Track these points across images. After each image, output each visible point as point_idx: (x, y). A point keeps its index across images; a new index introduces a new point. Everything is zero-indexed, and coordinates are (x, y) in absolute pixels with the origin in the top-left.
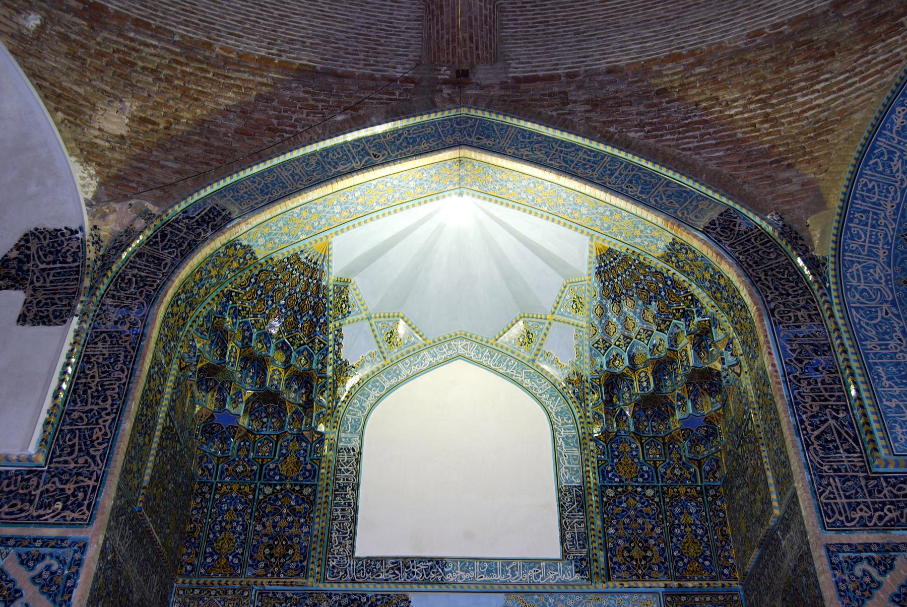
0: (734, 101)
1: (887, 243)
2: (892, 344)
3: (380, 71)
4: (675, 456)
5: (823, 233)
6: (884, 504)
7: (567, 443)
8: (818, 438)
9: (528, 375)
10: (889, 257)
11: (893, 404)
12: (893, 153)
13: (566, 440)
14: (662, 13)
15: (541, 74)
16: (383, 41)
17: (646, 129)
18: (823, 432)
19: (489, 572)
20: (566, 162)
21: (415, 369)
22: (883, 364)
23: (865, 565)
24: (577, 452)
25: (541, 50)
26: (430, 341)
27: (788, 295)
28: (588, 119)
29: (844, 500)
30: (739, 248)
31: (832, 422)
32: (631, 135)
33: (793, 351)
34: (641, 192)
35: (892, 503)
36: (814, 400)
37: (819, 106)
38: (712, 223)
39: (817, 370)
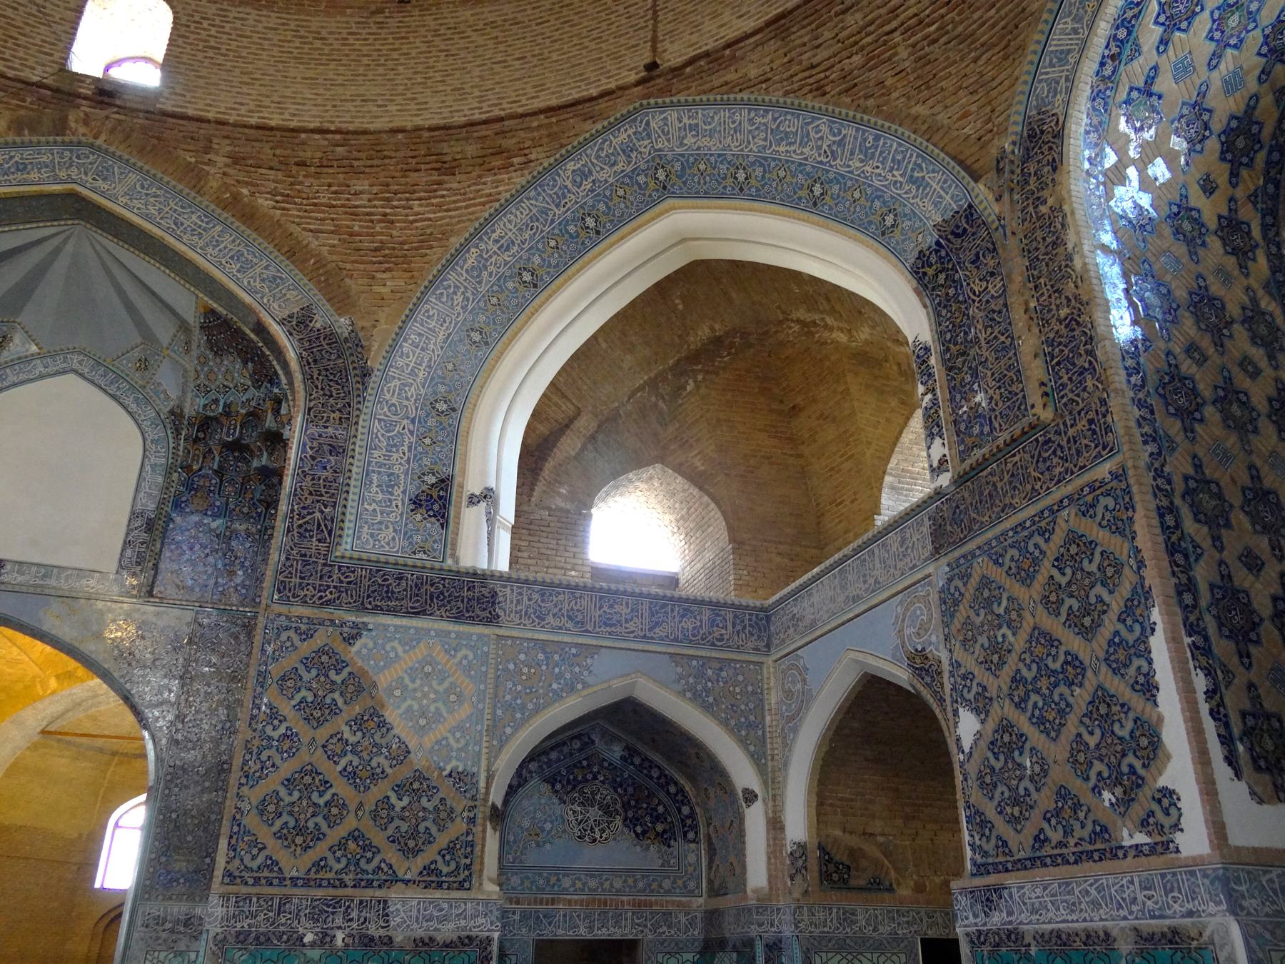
0: (361, 193)
1: (430, 367)
2: (395, 456)
3: (15, 69)
4: (249, 496)
5: (380, 347)
6: (329, 587)
7: (153, 470)
8: (300, 526)
9: (136, 400)
10: (426, 379)
11: (370, 508)
12: (458, 287)
13: (153, 467)
14: (331, 76)
15: (190, 112)
16: (28, 29)
17: (278, 198)
18: (307, 522)
19: (44, 576)
20: (176, 224)
21: (22, 377)
22: (379, 473)
23: (291, 633)
24: (160, 480)
25: (201, 82)
26: (45, 350)
27: (331, 396)
28: (224, 174)
29: (298, 580)
30: (306, 344)
31: (318, 514)
32: (260, 201)
33: (311, 448)
34: (238, 271)
35: (335, 587)
36: (311, 494)
37: (430, 219)
38: (291, 316)
39: (325, 468)
